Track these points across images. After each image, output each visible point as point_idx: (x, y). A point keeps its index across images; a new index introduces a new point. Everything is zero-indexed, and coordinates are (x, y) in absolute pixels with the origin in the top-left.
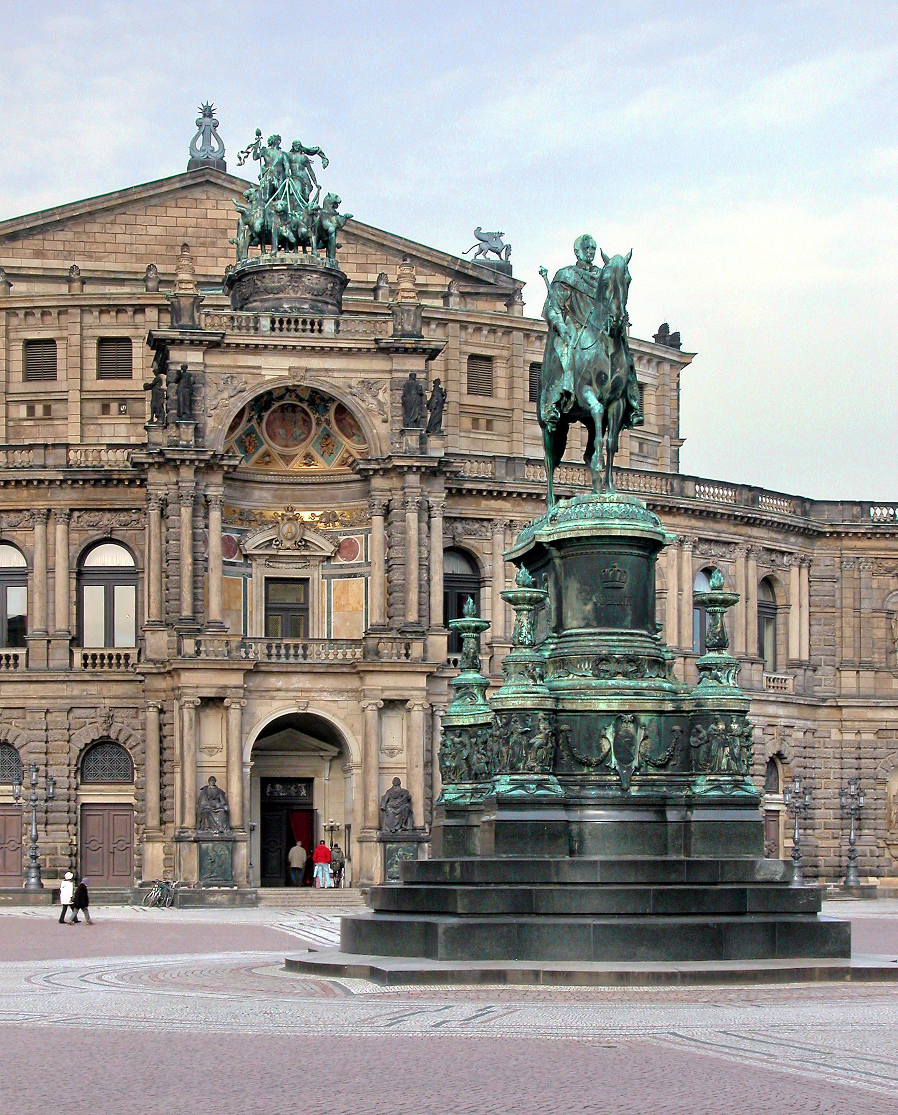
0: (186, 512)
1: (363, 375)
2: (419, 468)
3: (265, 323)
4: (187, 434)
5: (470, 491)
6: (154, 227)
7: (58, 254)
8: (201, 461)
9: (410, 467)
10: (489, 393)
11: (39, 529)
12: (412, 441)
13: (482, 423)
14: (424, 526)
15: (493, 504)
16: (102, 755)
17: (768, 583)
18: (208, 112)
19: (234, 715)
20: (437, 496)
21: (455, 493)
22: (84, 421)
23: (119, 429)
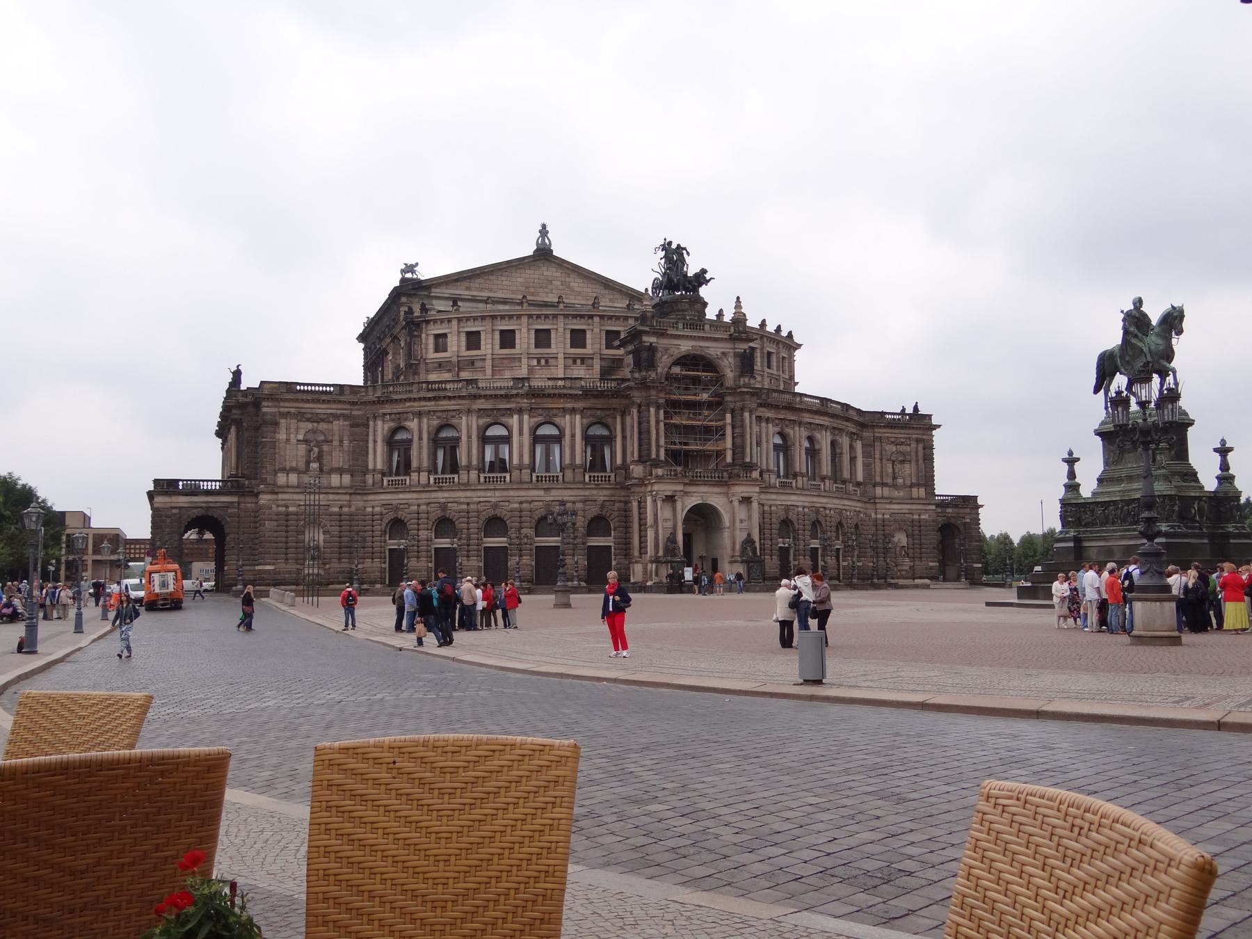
0: (652, 410)
3: (680, 326)
6: (519, 279)
7: (476, 289)
16: (598, 524)
17: (852, 447)
18: (544, 226)
19: (679, 505)
21: (760, 405)
22: (566, 367)
23: (579, 371)
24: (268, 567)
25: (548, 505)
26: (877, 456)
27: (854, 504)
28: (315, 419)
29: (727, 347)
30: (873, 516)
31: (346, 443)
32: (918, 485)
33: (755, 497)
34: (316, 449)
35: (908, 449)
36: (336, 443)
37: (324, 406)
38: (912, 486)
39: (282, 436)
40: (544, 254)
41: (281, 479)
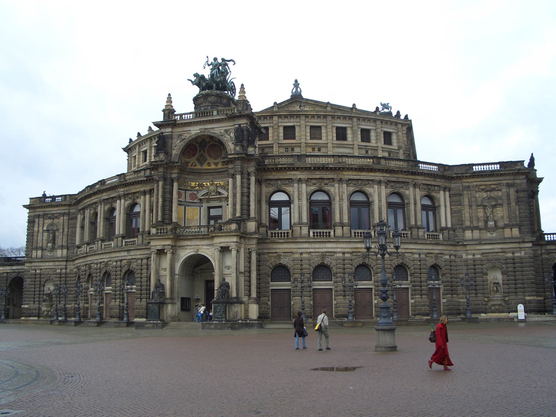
0: (161, 183)
1: (225, 128)
2: (238, 158)
4: (162, 156)
5: (281, 168)
8: (164, 164)
9: (235, 158)
10: (321, 139)
11: (142, 197)
12: (238, 148)
13: (316, 149)
14: (245, 180)
15: (292, 173)
18: (296, 81)
19: (169, 256)
20: (252, 169)
24: (26, 306)
25: (130, 262)
26: (466, 203)
27: (430, 247)
28: (53, 217)
29: (230, 126)
30: (464, 256)
31: (66, 230)
32: (511, 226)
33: (233, 246)
34: (51, 235)
35: (500, 194)
36: (61, 230)
37: (56, 209)
38: (505, 226)
39: (36, 229)
40: (296, 98)
41: (34, 254)
